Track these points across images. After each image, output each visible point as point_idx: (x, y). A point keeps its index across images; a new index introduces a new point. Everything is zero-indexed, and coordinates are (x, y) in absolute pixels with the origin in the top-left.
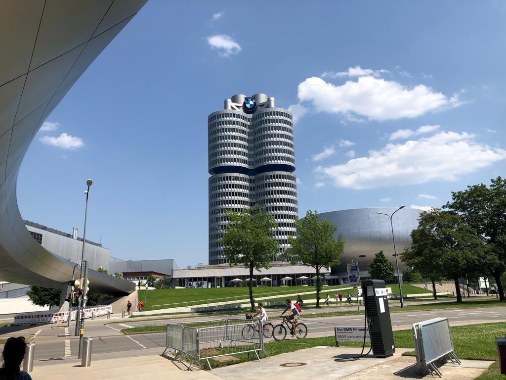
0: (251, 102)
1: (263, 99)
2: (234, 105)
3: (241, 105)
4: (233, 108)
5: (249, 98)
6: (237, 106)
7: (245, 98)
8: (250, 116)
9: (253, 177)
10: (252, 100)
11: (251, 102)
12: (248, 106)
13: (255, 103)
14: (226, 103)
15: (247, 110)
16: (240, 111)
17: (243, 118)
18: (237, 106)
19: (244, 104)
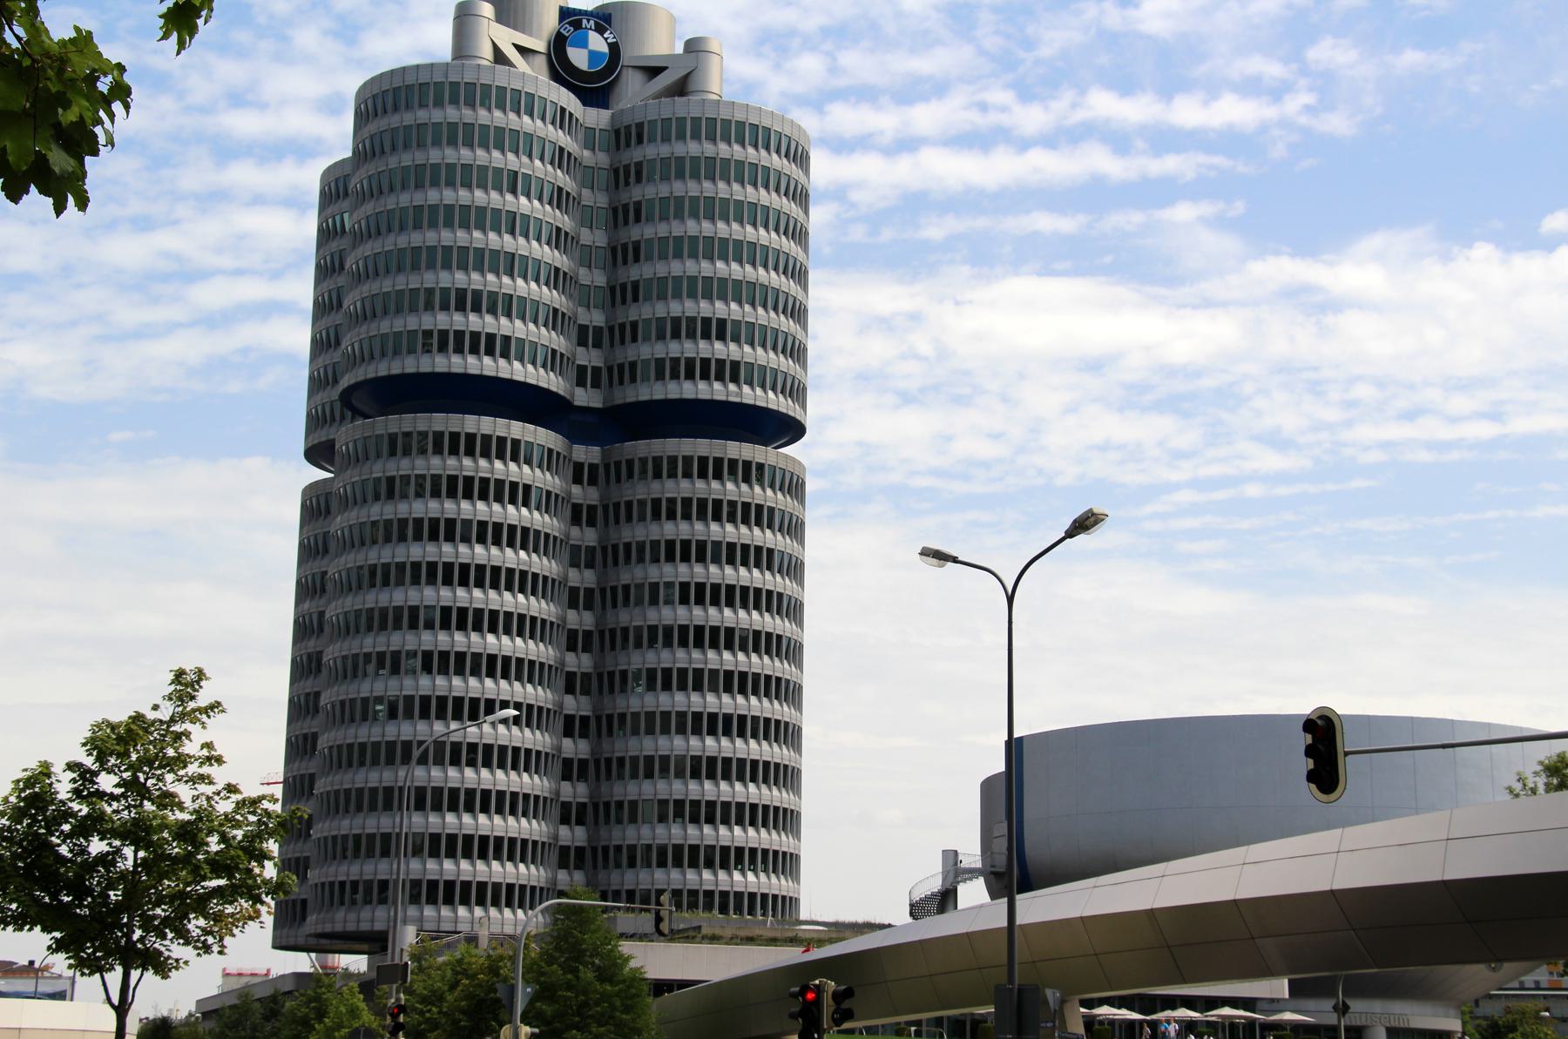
0: (598, 43)
1: (661, 43)
2: (506, 38)
3: (540, 45)
4: (499, 57)
6: (522, 50)
7: (565, 13)
8: (596, 118)
9: (587, 454)
10: (600, 30)
11: (598, 43)
12: (578, 58)
13: (614, 48)
17: (563, 118)
18: (522, 50)
19: (559, 43)
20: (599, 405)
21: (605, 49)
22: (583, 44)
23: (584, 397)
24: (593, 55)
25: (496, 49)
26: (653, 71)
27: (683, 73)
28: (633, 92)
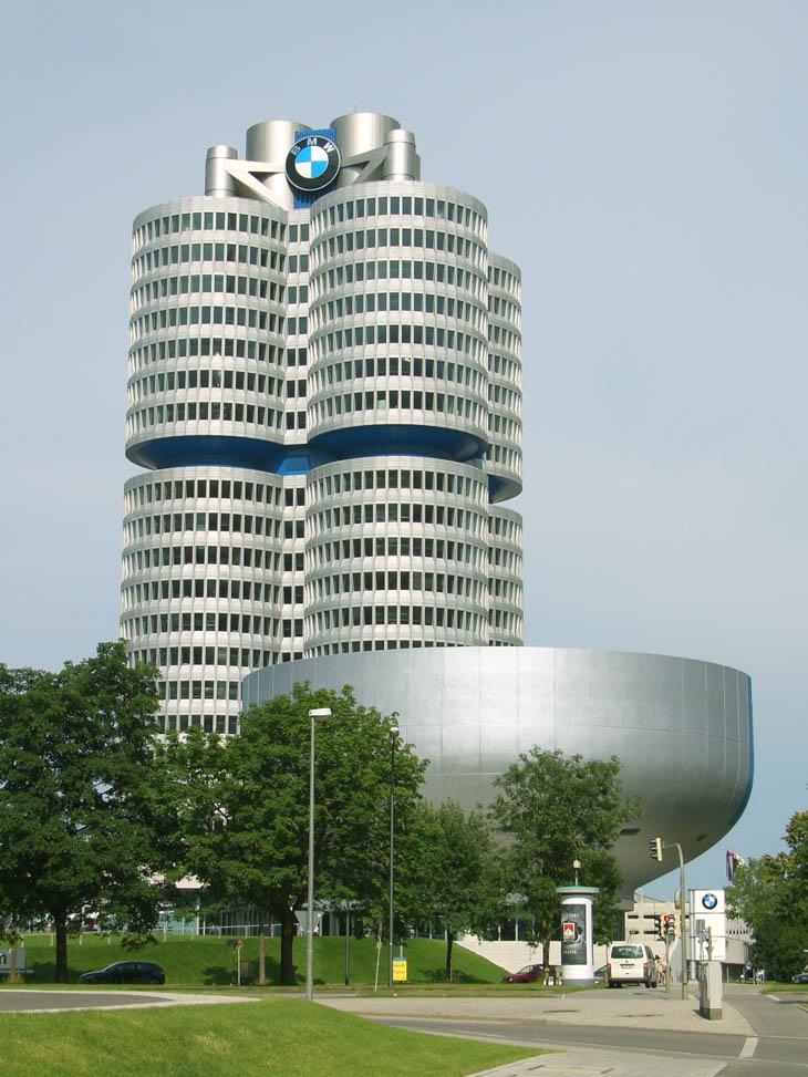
2: (243, 170)
3: (276, 162)
5: (316, 133)
10: (321, 143)
11: (319, 155)
12: (304, 170)
13: (333, 156)
14: (210, 159)
15: (306, 192)
16: (277, 192)
19: (291, 160)
20: (305, 442)
21: (326, 158)
22: (308, 159)
23: (295, 437)
24: (314, 164)
25: (233, 179)
26: (361, 165)
27: (379, 163)
28: (356, 188)
